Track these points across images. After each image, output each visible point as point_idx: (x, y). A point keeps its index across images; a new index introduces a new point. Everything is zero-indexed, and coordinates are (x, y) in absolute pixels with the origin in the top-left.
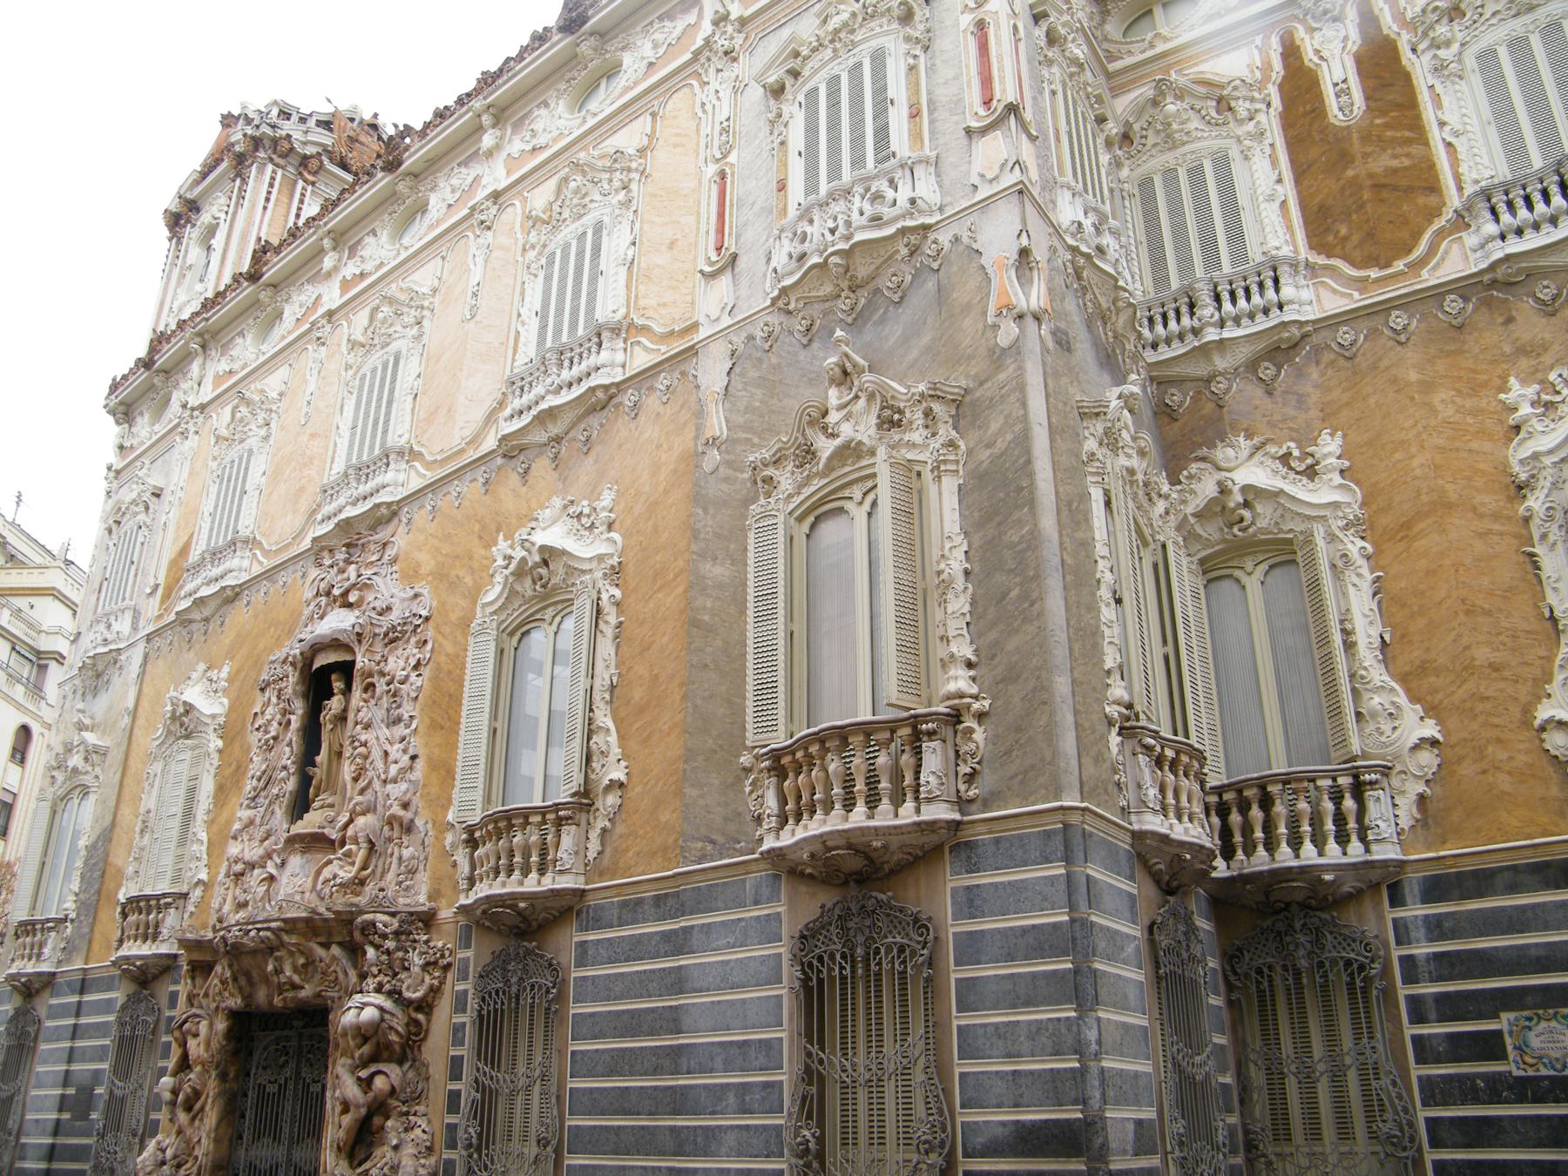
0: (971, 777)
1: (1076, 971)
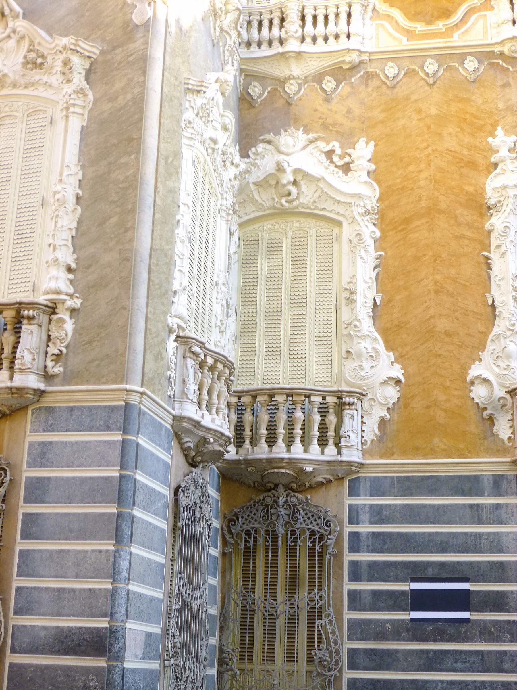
0: (58, 357)
1: (119, 515)
